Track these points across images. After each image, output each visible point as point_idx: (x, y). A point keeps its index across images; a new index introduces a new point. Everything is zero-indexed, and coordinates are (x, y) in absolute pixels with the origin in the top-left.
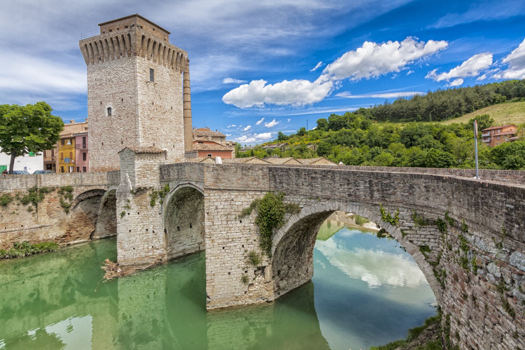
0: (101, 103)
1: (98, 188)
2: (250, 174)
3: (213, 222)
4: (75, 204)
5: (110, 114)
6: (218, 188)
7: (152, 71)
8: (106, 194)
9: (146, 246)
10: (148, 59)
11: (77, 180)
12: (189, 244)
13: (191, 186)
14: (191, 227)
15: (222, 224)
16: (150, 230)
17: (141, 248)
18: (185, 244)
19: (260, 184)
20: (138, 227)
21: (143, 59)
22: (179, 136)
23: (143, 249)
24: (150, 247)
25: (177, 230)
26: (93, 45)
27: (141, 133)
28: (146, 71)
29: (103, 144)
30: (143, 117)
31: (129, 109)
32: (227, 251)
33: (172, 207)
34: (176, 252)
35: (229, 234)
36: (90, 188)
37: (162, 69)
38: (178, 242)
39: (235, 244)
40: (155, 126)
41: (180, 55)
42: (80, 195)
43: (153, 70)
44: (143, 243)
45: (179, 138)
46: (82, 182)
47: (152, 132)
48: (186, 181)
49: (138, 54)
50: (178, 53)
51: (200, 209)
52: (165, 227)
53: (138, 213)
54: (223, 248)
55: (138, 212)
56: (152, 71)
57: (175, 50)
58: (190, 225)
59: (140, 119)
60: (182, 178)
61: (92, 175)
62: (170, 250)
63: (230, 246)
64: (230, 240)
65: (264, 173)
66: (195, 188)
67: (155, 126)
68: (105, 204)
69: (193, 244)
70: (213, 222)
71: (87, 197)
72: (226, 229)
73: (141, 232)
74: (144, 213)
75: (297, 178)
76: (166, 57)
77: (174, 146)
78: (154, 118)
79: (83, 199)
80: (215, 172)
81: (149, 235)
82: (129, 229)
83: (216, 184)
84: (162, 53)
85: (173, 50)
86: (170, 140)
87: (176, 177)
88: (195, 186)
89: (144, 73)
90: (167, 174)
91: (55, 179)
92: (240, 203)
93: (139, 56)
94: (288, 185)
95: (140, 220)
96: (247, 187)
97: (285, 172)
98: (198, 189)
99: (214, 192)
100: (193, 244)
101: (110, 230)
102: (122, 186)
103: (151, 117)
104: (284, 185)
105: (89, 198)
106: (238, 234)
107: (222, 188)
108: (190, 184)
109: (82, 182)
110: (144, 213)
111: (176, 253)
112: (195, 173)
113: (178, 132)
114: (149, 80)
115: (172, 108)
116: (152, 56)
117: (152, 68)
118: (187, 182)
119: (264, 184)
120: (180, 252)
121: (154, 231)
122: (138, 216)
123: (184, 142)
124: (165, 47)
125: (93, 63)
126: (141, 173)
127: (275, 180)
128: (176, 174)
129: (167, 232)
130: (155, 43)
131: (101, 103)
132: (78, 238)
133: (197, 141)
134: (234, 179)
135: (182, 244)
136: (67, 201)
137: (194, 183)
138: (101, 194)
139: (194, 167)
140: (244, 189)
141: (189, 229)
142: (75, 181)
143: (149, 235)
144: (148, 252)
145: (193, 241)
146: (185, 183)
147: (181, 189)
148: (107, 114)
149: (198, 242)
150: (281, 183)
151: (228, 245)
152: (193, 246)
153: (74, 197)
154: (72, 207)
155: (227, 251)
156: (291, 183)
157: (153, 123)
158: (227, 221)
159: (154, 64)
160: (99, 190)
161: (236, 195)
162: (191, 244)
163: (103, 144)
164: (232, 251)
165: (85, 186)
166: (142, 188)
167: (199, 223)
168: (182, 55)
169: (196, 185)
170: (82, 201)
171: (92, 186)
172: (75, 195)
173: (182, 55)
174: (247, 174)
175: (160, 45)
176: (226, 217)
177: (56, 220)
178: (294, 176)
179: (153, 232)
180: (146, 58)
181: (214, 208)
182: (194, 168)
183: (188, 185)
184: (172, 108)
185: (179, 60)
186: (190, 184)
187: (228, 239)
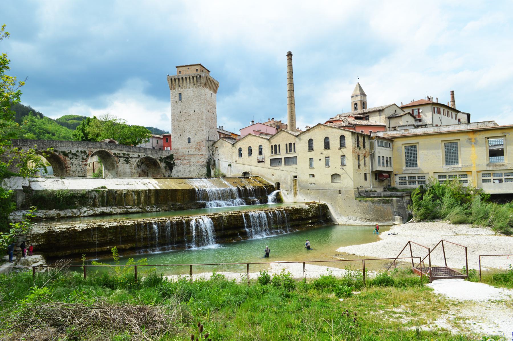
7: (180, 95)
21: (175, 90)
45: (201, 129)
47: (179, 128)
50: (196, 77)
56: (180, 95)
57: (194, 76)
77: (196, 134)
86: (193, 131)
114: (178, 100)
115: (195, 111)
117: (180, 93)
130: (179, 79)
168: (200, 76)
175: (182, 78)
184: (195, 111)
185: (198, 80)
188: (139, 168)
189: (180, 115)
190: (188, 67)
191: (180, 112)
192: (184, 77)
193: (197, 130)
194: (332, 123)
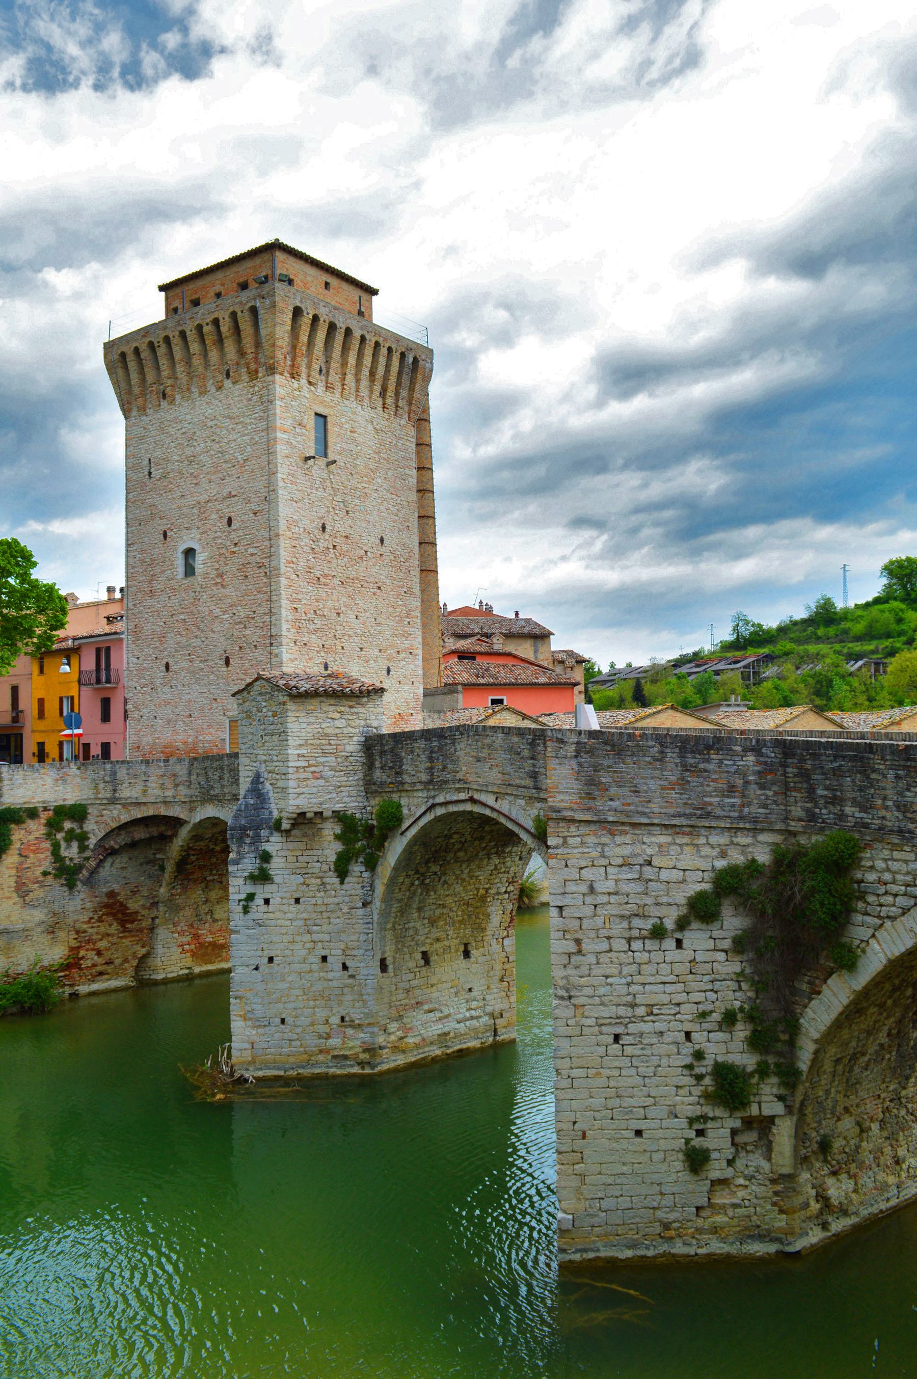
0: (165, 535)
1: (163, 811)
2: (711, 767)
3: (578, 942)
4: (93, 863)
5: (190, 571)
6: (595, 819)
8: (184, 833)
9: (321, 1014)
10: (310, 383)
11: (102, 786)
12: (460, 1016)
13: (477, 809)
14: (467, 954)
15: (611, 950)
16: (335, 962)
17: (304, 1021)
18: (447, 1016)
19: (749, 804)
20: (299, 946)
21: (296, 385)
22: (407, 636)
23: (312, 1024)
24: (335, 1020)
25: (422, 962)
26: (145, 354)
27: (288, 630)
28: (305, 421)
29: (167, 666)
30: (294, 577)
31: (251, 550)
32: (629, 1050)
33: (407, 881)
34: (417, 1040)
35: (634, 988)
36: (138, 814)
37: (354, 413)
38: (426, 1007)
39: (659, 1026)
40: (330, 604)
41: (411, 360)
42: (107, 836)
43: (325, 417)
44: (311, 1003)
46: (115, 791)
48: (459, 790)
49: (280, 369)
50: (403, 355)
51: (498, 893)
52: (384, 952)
53: (297, 901)
54: (617, 1038)
55: (297, 896)
57: (394, 346)
58: (462, 948)
59: (284, 581)
60: (446, 782)
61: (143, 768)
62: (400, 1034)
63: (641, 1035)
64: (641, 1011)
65: (765, 763)
66: (494, 815)
67: (330, 604)
68: (182, 865)
69: (472, 1018)
70: (578, 942)
71: (128, 840)
72: (626, 970)
73: (306, 967)
74: (313, 901)
75: (902, 784)
76: (366, 372)
77: (389, 671)
78: (326, 576)
79: (117, 847)
80: (585, 758)
81: (330, 975)
82: (268, 953)
83: (591, 803)
84: (352, 360)
85: (387, 345)
86: (376, 652)
87: (424, 777)
88: (493, 809)
89: (297, 430)
90: (391, 768)
91: (41, 782)
92: (677, 875)
93: (282, 374)
94: (864, 809)
95: (301, 923)
96: (701, 817)
97: (853, 759)
98: (502, 820)
99: (584, 829)
100: (472, 1018)
101: (194, 954)
102: (246, 805)
103: (318, 574)
104: (848, 810)
105: (133, 845)
106: (669, 988)
107: (611, 819)
108: (472, 800)
109: (115, 791)
110: (313, 901)
111: (417, 1046)
112: (494, 762)
113: (401, 621)
115: (382, 540)
116: (321, 371)
118: (463, 796)
119: (765, 806)
120: (432, 1043)
121: (348, 964)
122: (294, 908)
123: (420, 657)
124: (363, 339)
125: (143, 410)
126: (306, 764)
127: (811, 791)
128: (422, 767)
129: (391, 968)
130: (332, 327)
131: (165, 535)
132: (101, 974)
133: (453, 652)
134: (653, 785)
135: (439, 1015)
136: (71, 852)
137: (490, 800)
138: (169, 833)
139: (488, 741)
140: (689, 822)
141: (461, 963)
142: (96, 787)
143: (330, 975)
144: (328, 1037)
145: (474, 1004)
146: (455, 798)
147: (438, 819)
148: (181, 570)
149: (489, 1009)
150: (834, 800)
151: (632, 1028)
152: (474, 1022)
153: (92, 842)
154: (84, 872)
155: (629, 1050)
156: (880, 802)
157: (324, 595)
158: (629, 940)
159: (328, 397)
160: (165, 817)
161: (660, 846)
162: (468, 1015)
163: (167, 666)
164: (648, 1052)
165: (124, 806)
166: (309, 815)
167: (494, 943)
168: (415, 360)
169: (497, 806)
170: (113, 852)
171: (145, 804)
172: (95, 830)
173: (415, 360)
174: (701, 766)
175: (348, 332)
176: (625, 924)
177: (39, 915)
178: (891, 775)
179: (345, 967)
180: (304, 381)
181: (584, 888)
182: (489, 746)
183: (468, 807)
184: (382, 540)
186: (472, 800)
187: (633, 1005)
188: (71, 886)
189: (322, 544)
190: (326, 277)
191: (324, 528)
192: (357, 334)
193: (392, 646)
194: (474, 659)
